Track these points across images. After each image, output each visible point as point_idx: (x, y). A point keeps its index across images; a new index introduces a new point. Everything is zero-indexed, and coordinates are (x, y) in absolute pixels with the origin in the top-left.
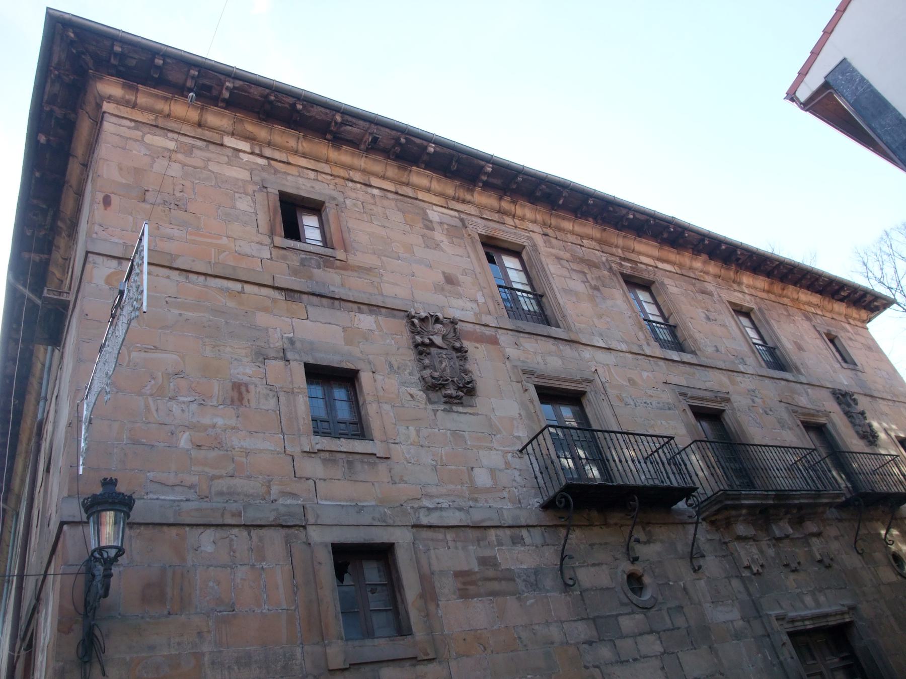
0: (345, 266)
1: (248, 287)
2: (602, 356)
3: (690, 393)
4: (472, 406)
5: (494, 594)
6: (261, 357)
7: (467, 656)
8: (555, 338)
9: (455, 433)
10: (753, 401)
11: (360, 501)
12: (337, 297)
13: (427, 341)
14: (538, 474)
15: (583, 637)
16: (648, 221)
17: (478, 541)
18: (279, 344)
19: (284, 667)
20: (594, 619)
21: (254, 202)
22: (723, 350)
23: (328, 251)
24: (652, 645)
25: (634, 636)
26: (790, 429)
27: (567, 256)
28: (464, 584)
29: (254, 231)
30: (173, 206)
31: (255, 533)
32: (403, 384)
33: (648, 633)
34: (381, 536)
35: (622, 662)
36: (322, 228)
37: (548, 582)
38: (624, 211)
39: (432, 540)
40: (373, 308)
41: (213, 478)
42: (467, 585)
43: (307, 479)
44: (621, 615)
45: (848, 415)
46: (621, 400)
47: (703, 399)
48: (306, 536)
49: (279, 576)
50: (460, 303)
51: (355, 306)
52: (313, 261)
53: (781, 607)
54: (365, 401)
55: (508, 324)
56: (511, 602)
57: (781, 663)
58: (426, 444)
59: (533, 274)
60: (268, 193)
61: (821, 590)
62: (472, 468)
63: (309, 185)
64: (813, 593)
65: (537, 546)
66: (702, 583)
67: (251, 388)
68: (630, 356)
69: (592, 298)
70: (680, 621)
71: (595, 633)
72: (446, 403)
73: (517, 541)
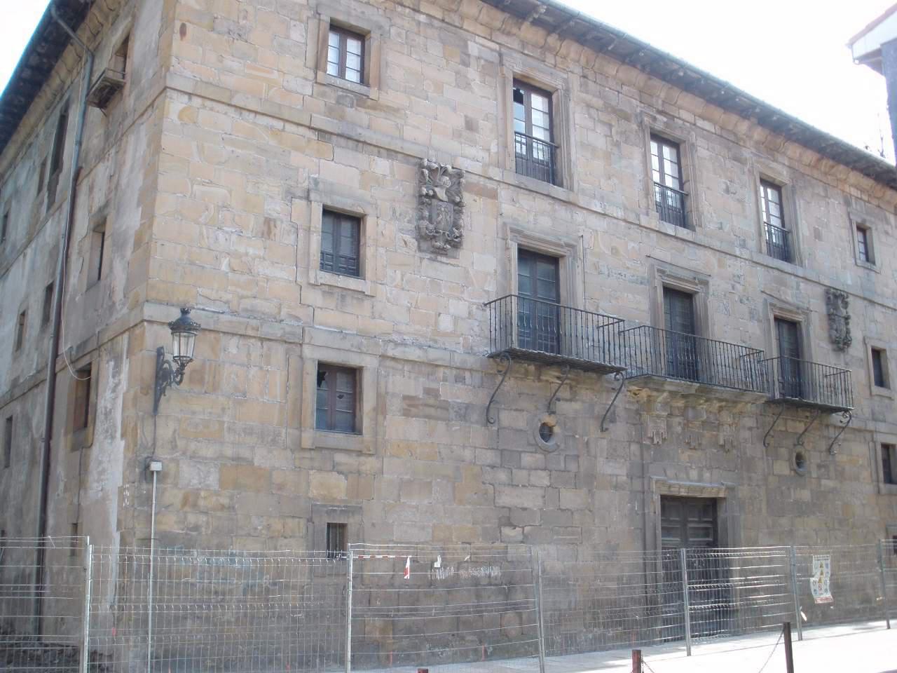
0: (376, 107)
1: (289, 127)
2: (593, 221)
3: (668, 269)
4: (455, 258)
5: (429, 417)
6: (290, 195)
7: (398, 457)
8: (554, 198)
9: (433, 280)
10: (733, 288)
11: (346, 329)
12: (362, 139)
13: (431, 193)
14: (493, 329)
15: (489, 461)
16: (699, 80)
17: (428, 375)
18: (305, 185)
19: (272, 440)
20: (502, 451)
21: (306, 31)
22: (727, 228)
23: (363, 89)
24: (543, 479)
25: (530, 469)
26: (759, 321)
27: (598, 103)
28: (409, 406)
29: (303, 63)
30: (236, 36)
31: (266, 344)
32: (401, 230)
33: (542, 470)
34: (353, 360)
35: (513, 485)
36: (363, 56)
37: (475, 417)
38: (676, 67)
39: (393, 368)
40: (391, 153)
41: (242, 297)
42: (411, 406)
43: (309, 306)
44: (525, 452)
45: (831, 317)
46: (596, 266)
47: (680, 279)
48: (301, 351)
49: (278, 378)
50: (472, 151)
51: (376, 150)
52: (348, 99)
53: (666, 475)
54: (365, 243)
55: (512, 178)
56: (441, 426)
57: (644, 514)
58: (407, 288)
59: (556, 121)
60: (320, 20)
61: (710, 468)
62: (440, 314)
63: (359, 10)
64: (701, 470)
65: (474, 387)
66: (605, 442)
67: (278, 223)
68: (624, 224)
69: (608, 156)
70: (572, 467)
71: (499, 461)
72: (432, 252)
73: (459, 379)
